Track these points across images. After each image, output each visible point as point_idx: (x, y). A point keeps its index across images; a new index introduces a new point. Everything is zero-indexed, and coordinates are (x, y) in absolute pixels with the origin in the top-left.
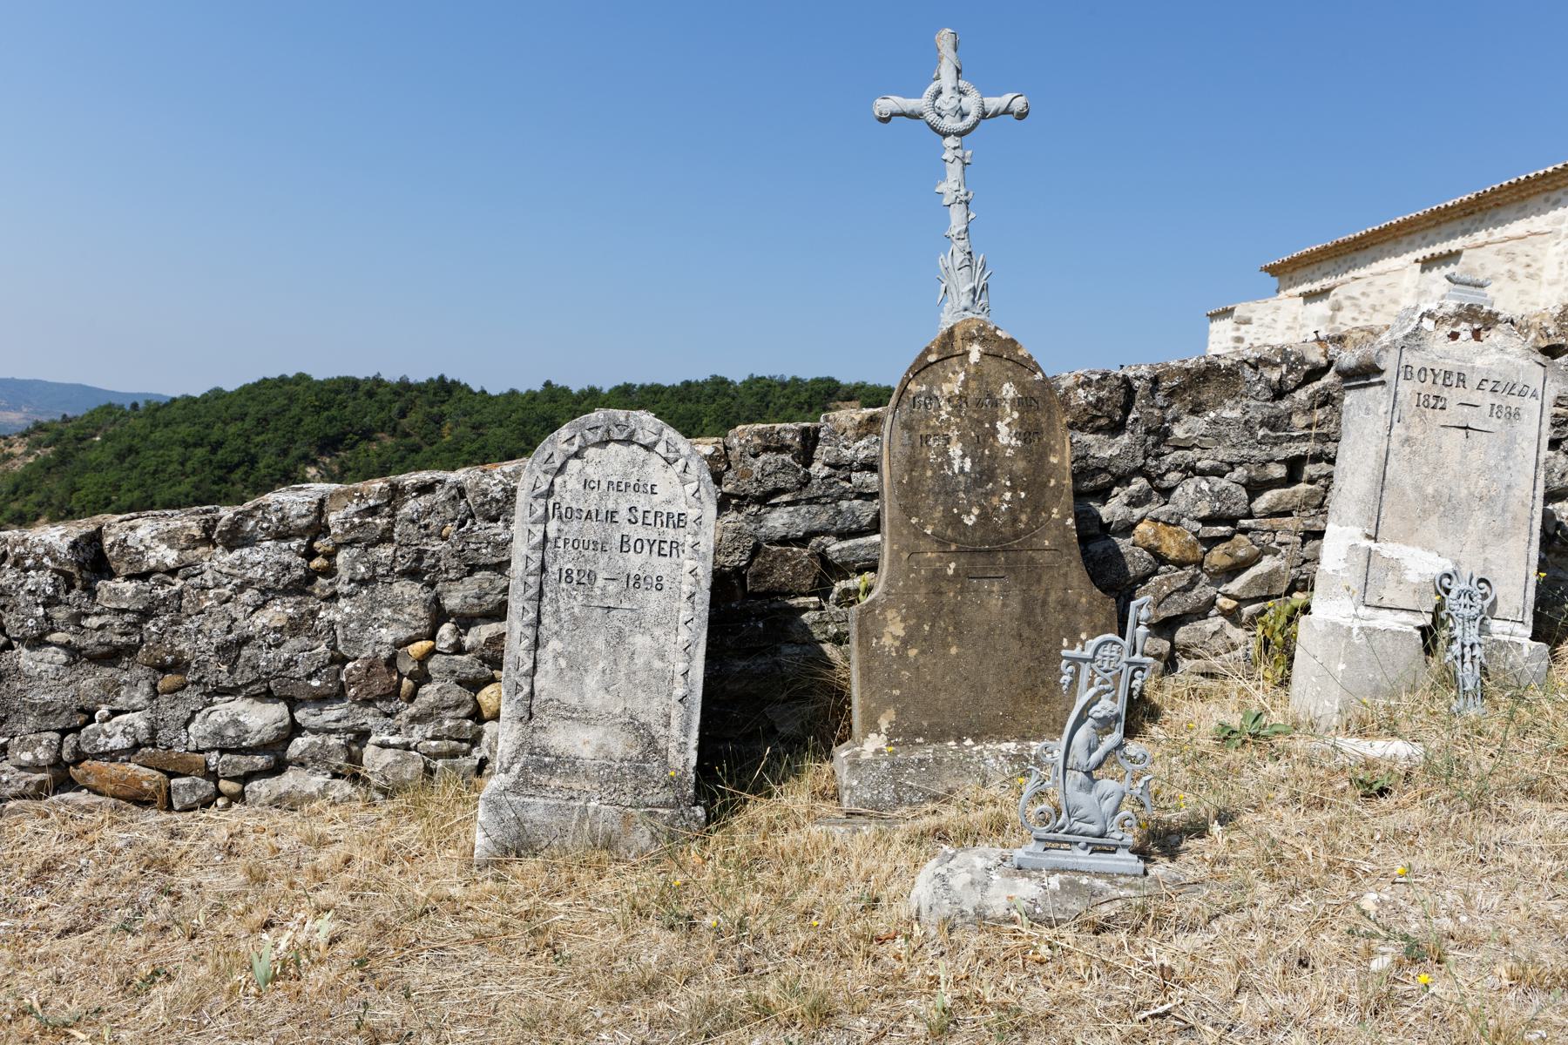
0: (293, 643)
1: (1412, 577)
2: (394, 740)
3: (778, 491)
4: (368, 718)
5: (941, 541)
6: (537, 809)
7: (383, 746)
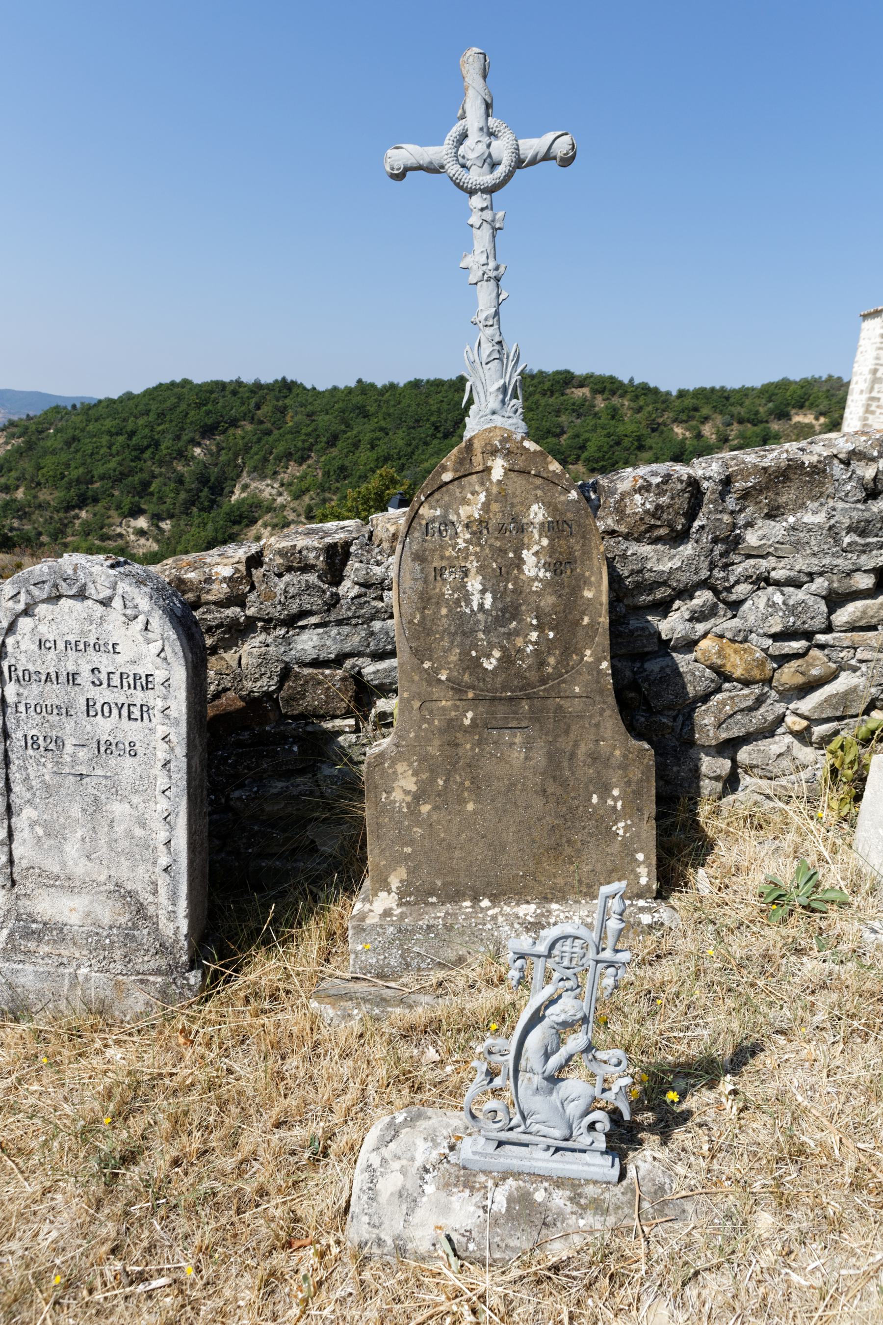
3: (304, 614)
5: (457, 688)
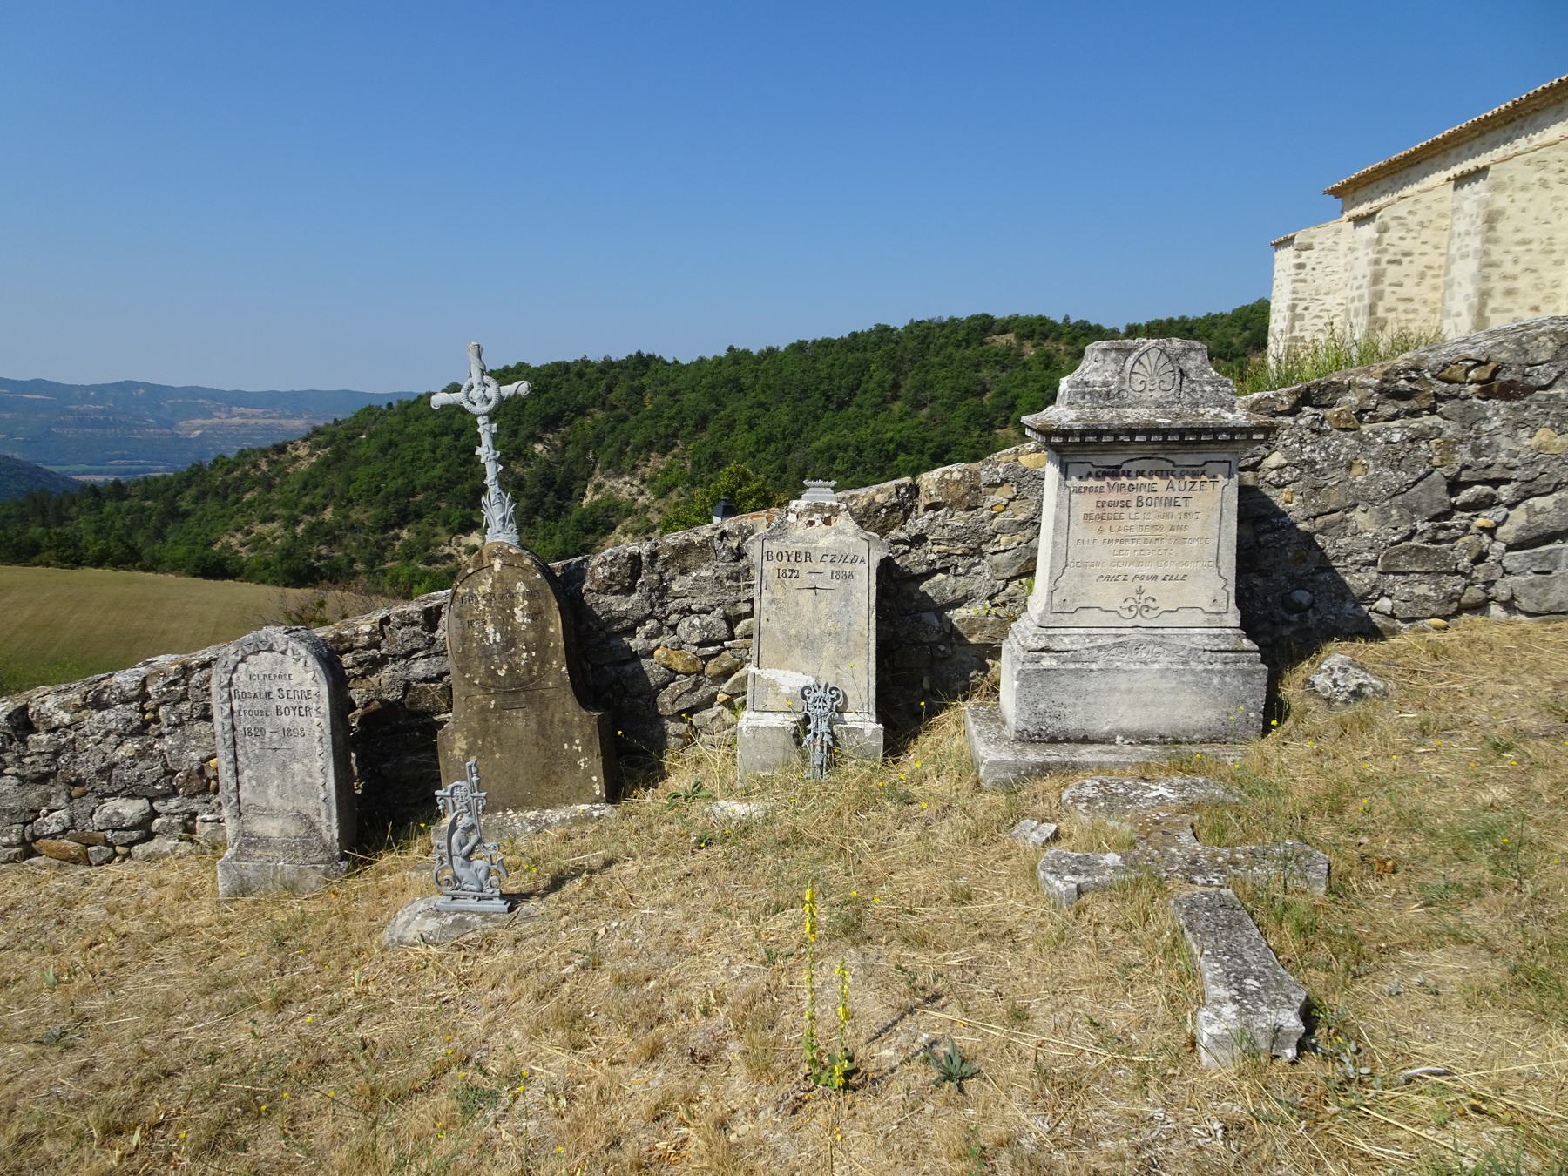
0: (141, 765)
1: (785, 690)
2: (209, 818)
3: (415, 651)
4: (195, 804)
5: (485, 687)
6: (249, 867)
7: (204, 821)
